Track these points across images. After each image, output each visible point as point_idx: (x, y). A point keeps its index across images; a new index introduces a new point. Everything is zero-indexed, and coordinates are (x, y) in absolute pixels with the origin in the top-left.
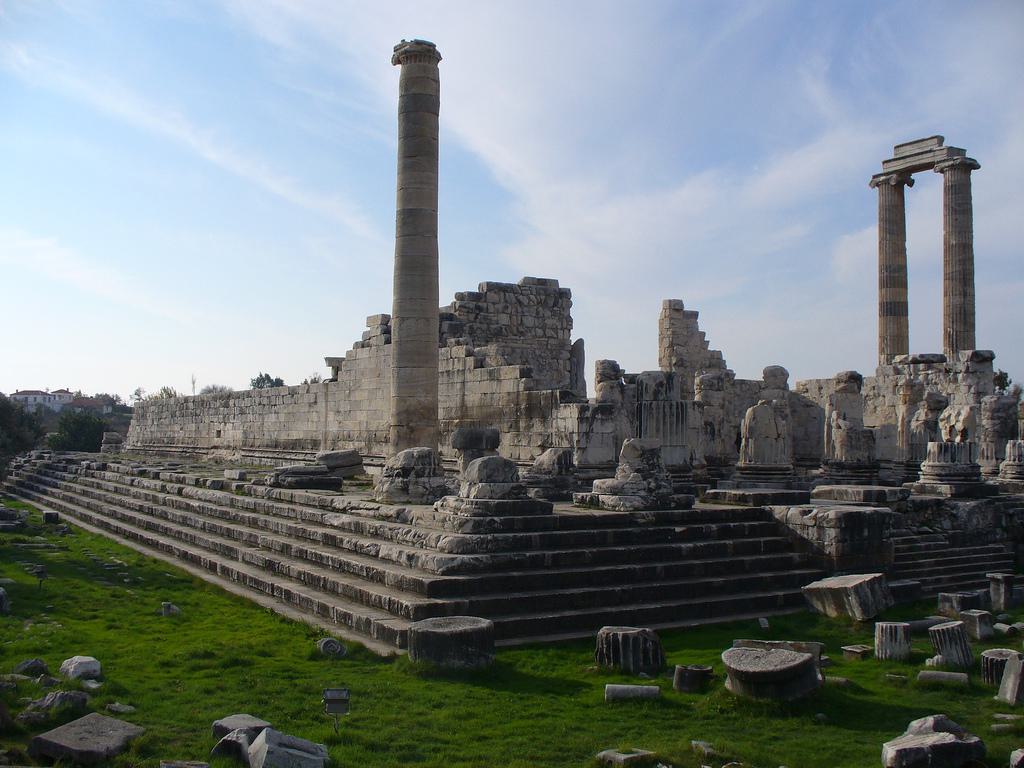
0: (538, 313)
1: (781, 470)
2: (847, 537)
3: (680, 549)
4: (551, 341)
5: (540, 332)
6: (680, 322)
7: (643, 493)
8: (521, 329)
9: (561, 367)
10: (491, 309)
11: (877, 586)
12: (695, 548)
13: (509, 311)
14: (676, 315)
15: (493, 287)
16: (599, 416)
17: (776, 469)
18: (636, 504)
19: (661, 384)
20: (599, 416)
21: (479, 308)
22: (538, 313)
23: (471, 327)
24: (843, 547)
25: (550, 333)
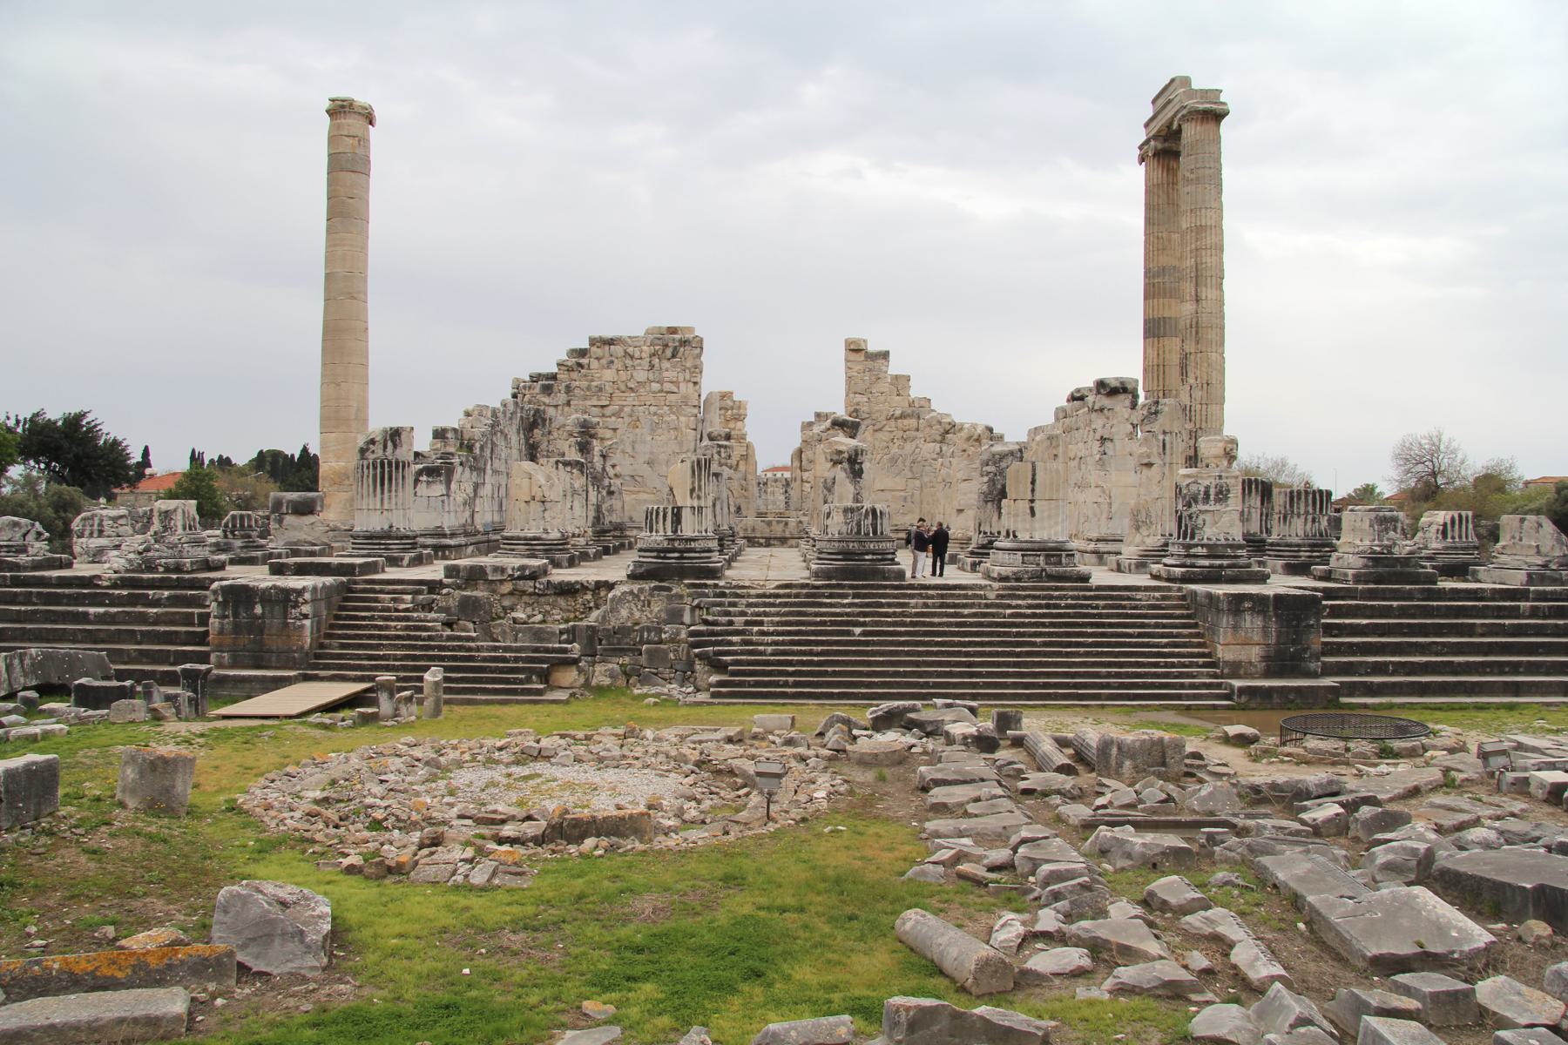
0: (652, 367)
1: (525, 539)
2: (229, 612)
3: (86, 614)
4: (672, 397)
5: (655, 386)
6: (865, 359)
7: (132, 556)
8: (631, 385)
9: (683, 425)
10: (594, 364)
11: (16, 662)
12: (106, 613)
13: (618, 364)
14: (860, 357)
15: (593, 341)
16: (424, 478)
17: (519, 538)
18: (115, 566)
19: (373, 442)
20: (424, 478)
21: (580, 365)
22: (652, 367)
23: (568, 387)
24: (222, 625)
25: (668, 387)
